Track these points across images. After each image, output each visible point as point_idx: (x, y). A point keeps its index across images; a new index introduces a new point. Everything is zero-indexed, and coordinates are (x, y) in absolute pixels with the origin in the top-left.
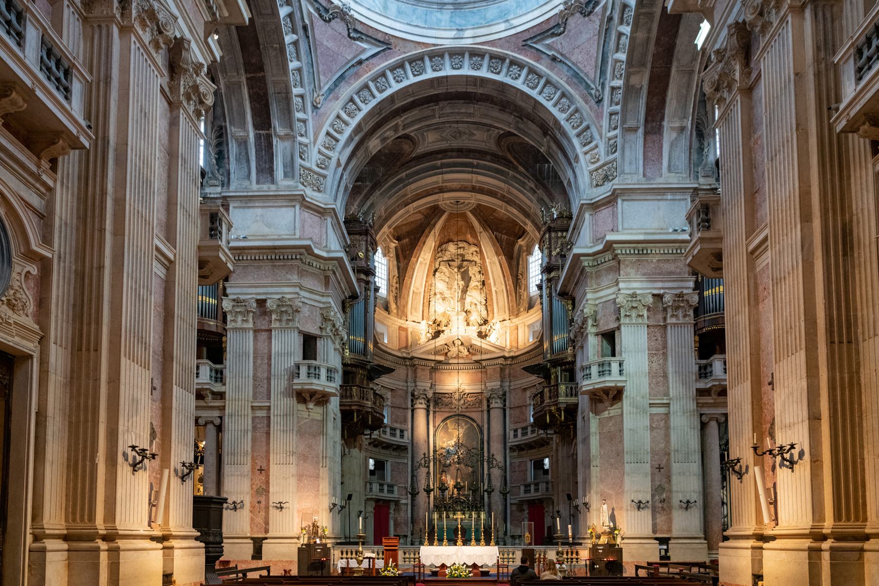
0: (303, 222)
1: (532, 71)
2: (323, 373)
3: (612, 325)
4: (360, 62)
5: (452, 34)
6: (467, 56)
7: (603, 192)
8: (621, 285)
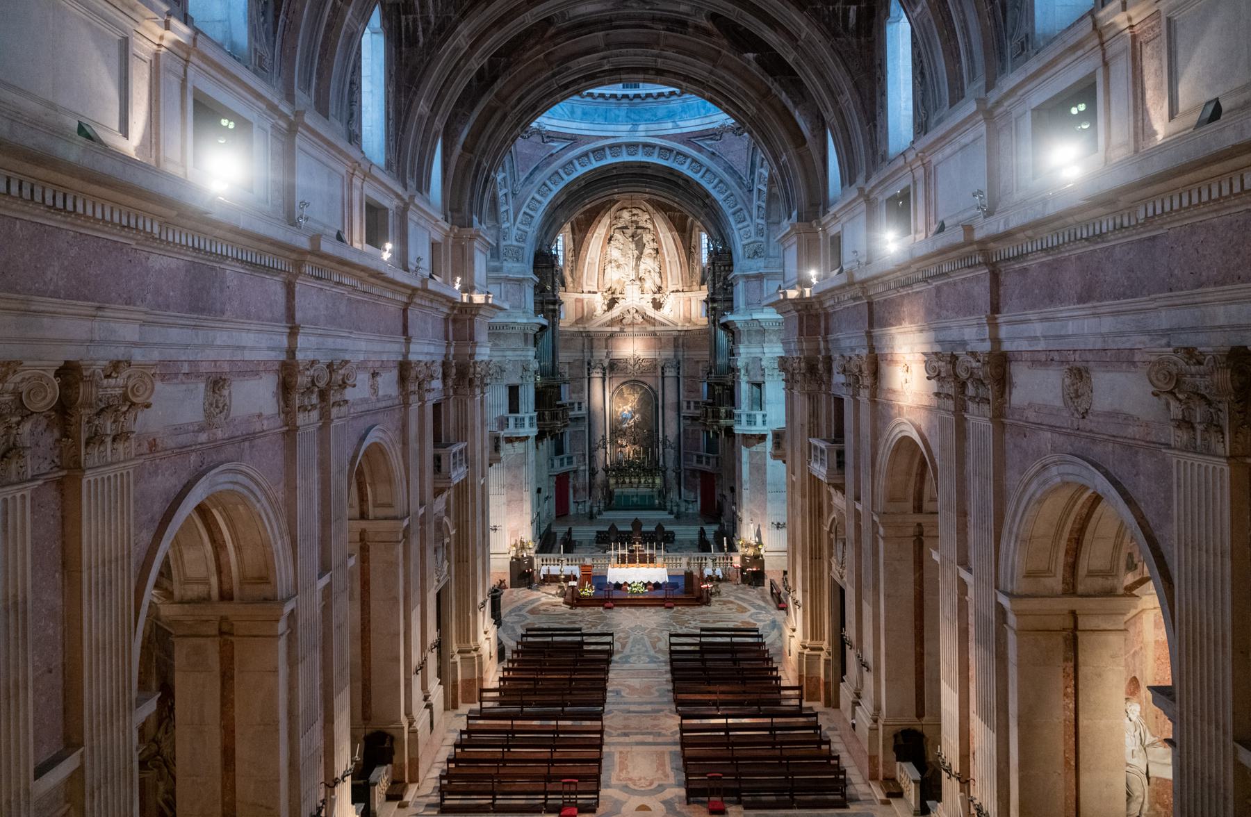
0: (507, 292)
1: (694, 160)
2: (527, 422)
3: (759, 379)
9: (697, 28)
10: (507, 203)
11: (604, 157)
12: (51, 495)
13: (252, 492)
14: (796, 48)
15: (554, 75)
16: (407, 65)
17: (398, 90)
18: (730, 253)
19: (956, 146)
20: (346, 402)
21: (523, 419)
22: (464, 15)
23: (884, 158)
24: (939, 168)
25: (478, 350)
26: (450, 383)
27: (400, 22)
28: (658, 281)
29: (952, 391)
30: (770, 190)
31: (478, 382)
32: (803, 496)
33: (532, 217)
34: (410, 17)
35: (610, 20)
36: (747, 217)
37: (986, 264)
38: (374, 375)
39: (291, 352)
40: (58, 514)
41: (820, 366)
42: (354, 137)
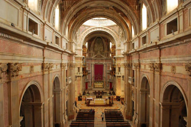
1: (109, 30)
2: (81, 73)
3: (120, 67)
8: (121, 62)
9: (111, 9)
10: (78, 37)
11: (95, 29)
12: (6, 85)
13: (37, 85)
14: (127, 12)
15: (87, 16)
16: (62, 14)
17: (61, 18)
18: (115, 46)
19: (154, 29)
20: (52, 70)
21: (80, 73)
22: (72, 6)
23: (142, 31)
24: (151, 33)
25: (73, 61)
26: (69, 67)
27: (61, 7)
28: (103, 50)
29: (153, 70)
30: (122, 35)
31: (73, 67)
32: (127, 86)
33: (82, 39)
34: (63, 6)
35: (96, 7)
37: (159, 49)
38: (57, 65)
39: (43, 61)
40: (7, 88)
41: (130, 65)
42: (54, 26)
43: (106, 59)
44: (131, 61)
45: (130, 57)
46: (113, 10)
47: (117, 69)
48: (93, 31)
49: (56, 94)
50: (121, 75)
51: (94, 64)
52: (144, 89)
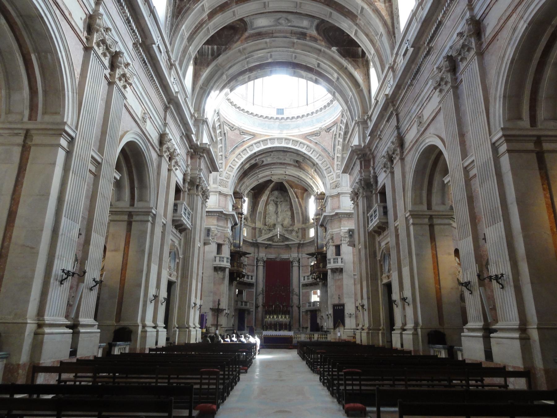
2: (225, 260)
3: (338, 243)
4: (244, 142)
5: (279, 132)
6: (284, 140)
7: (335, 192)
8: (342, 228)
10: (222, 159)
11: (267, 144)
17: (173, 16)
30: (343, 154)
32: (366, 248)
33: (233, 168)
36: (332, 170)
41: (372, 180)
43: (299, 244)
44: (374, 169)
45: (369, 161)
46: (315, 40)
47: (331, 253)
48: (262, 147)
49: (133, 223)
50: (343, 265)
51: (265, 259)
52: (425, 207)
